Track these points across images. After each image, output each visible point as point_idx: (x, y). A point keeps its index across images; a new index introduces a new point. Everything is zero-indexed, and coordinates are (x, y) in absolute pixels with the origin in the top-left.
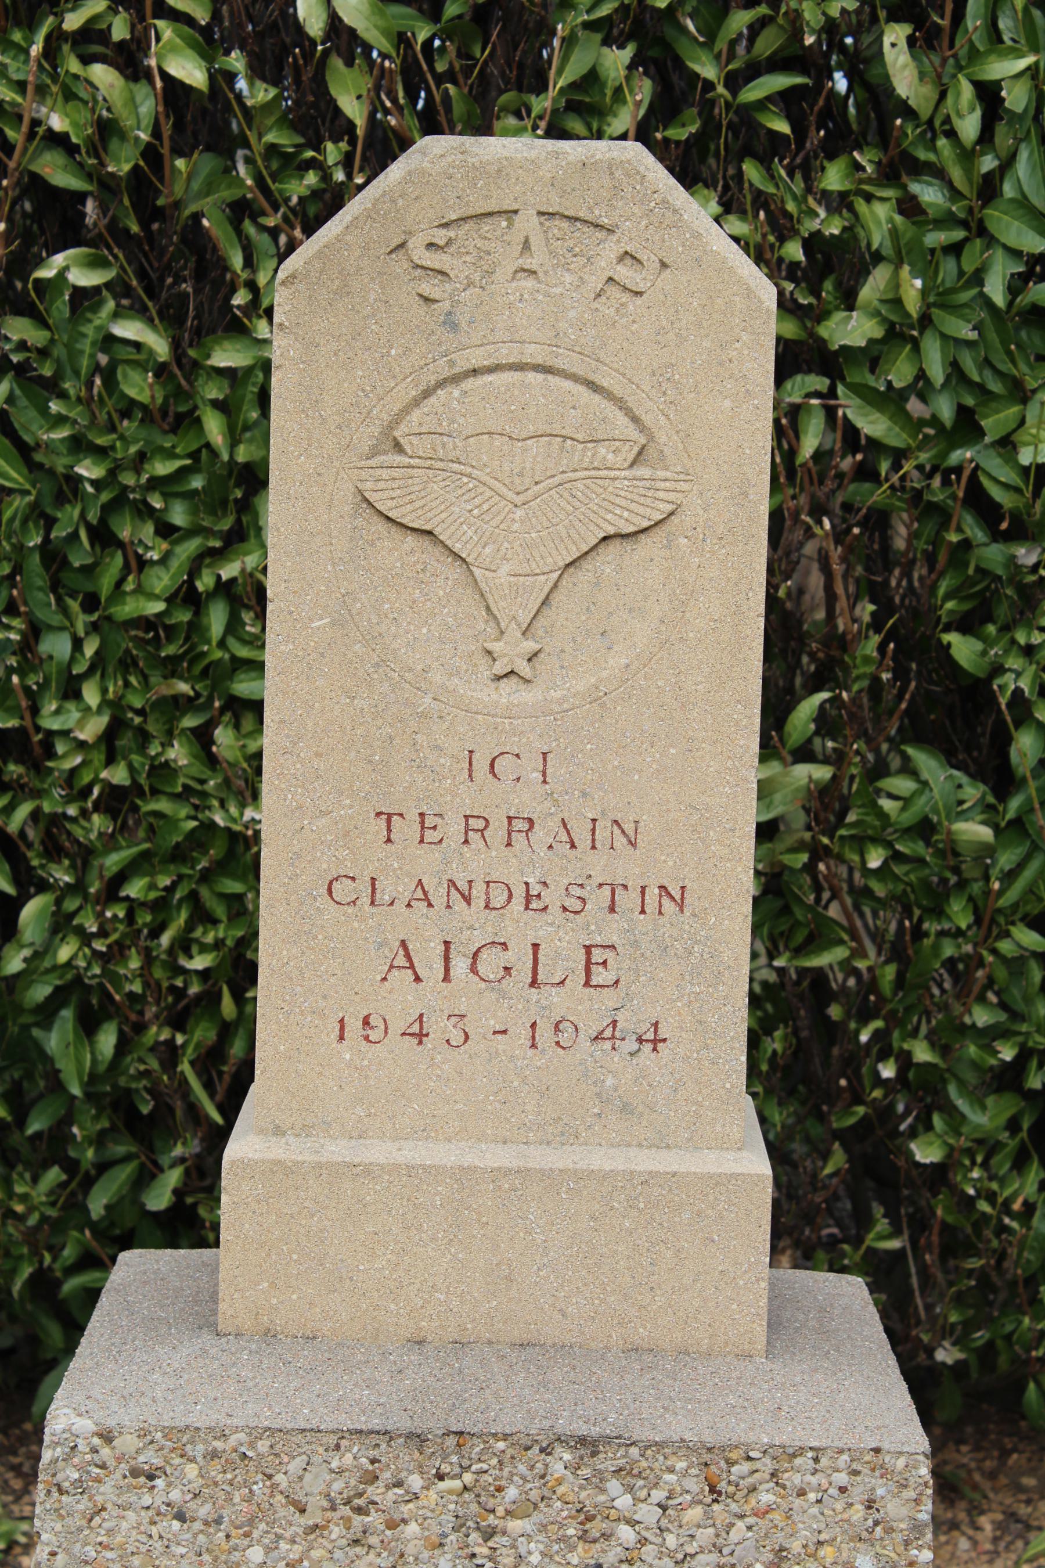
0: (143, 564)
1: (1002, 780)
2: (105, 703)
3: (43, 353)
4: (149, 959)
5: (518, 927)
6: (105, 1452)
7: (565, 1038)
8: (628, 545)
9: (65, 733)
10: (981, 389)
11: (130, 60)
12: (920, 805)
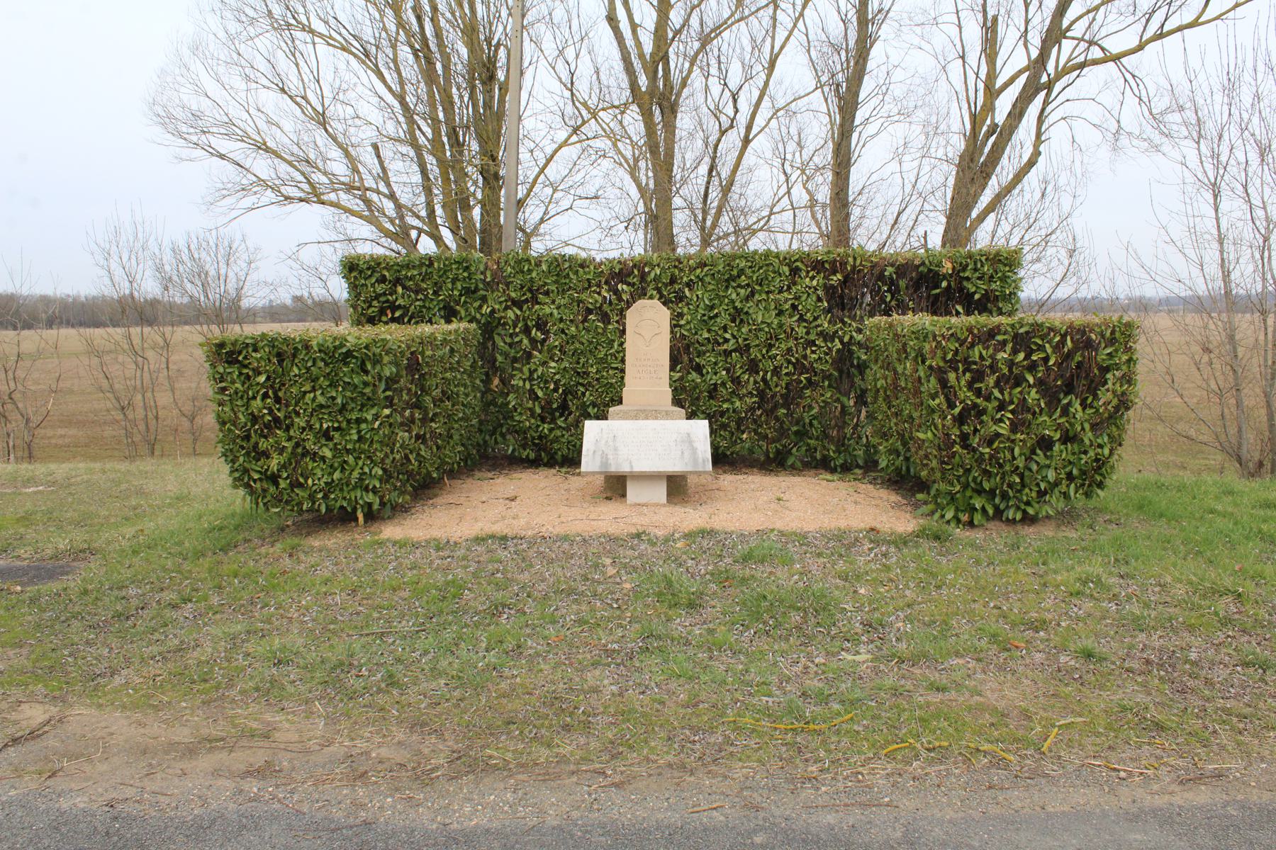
1: (702, 375)
11: (599, 293)
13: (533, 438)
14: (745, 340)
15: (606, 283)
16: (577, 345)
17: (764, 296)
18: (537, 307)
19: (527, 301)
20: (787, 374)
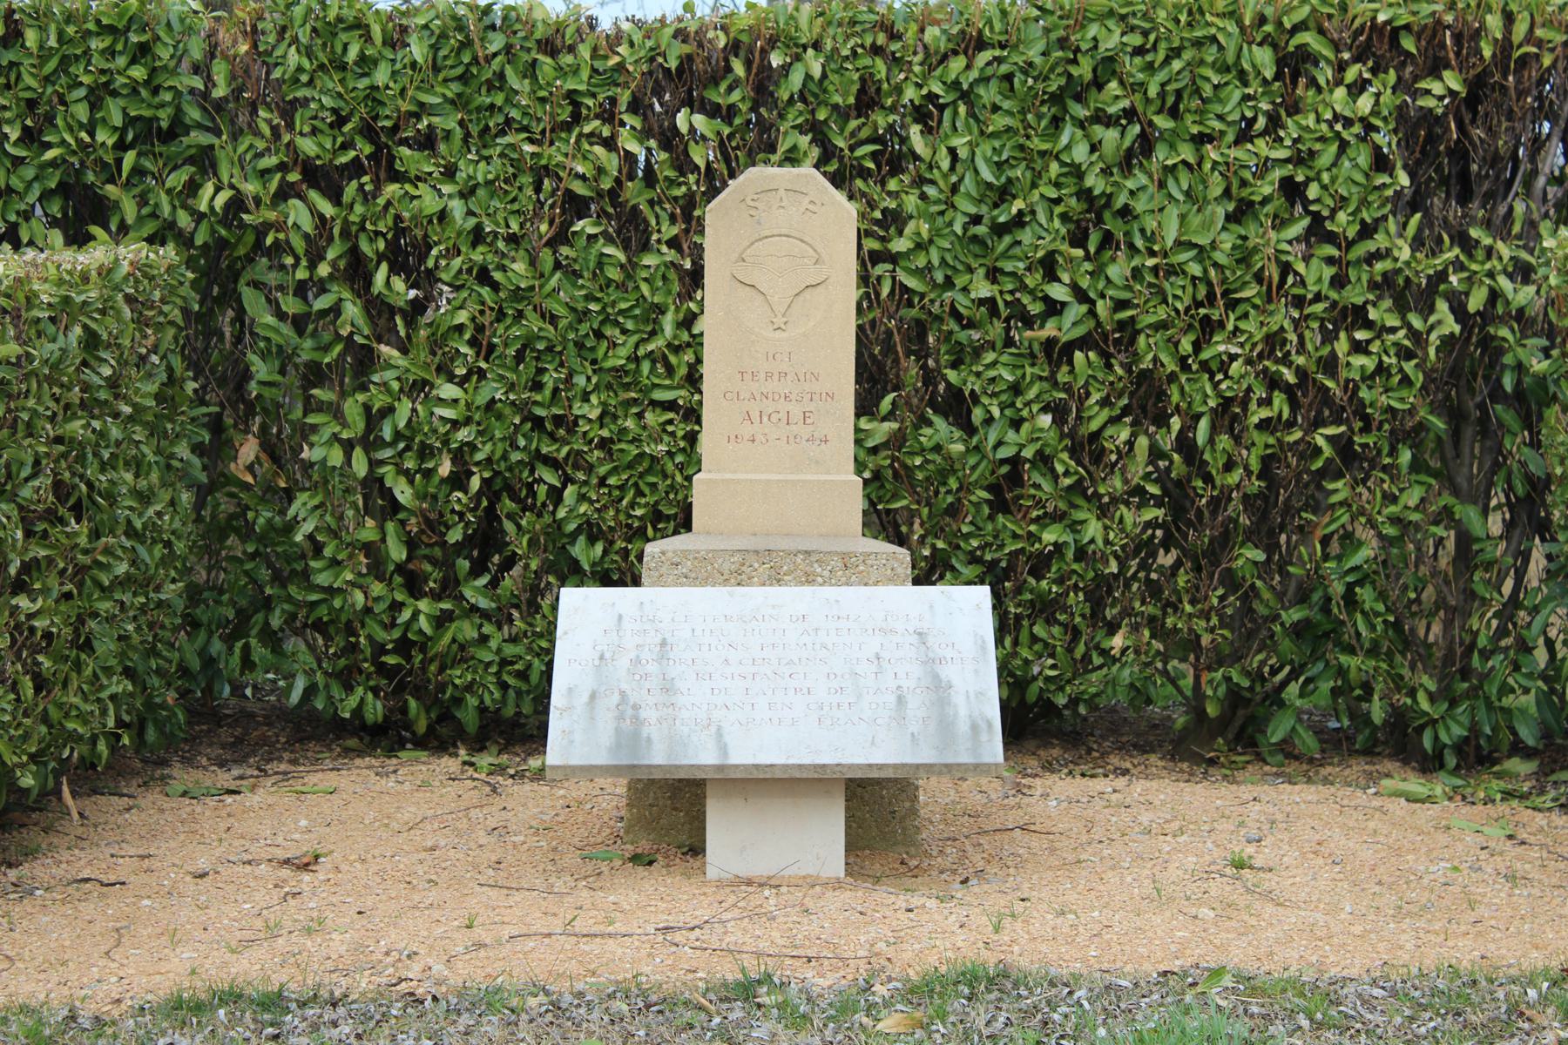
0: (615, 345)
1: (970, 430)
2: (601, 403)
3: (575, 260)
4: (618, 511)
5: (783, 406)
9: (584, 416)
10: (954, 268)
11: (610, 144)
12: (936, 438)
13: (380, 649)
14: (1121, 305)
15: (635, 106)
16: (534, 323)
17: (1187, 153)
18: (392, 189)
19: (356, 169)
20: (1264, 425)
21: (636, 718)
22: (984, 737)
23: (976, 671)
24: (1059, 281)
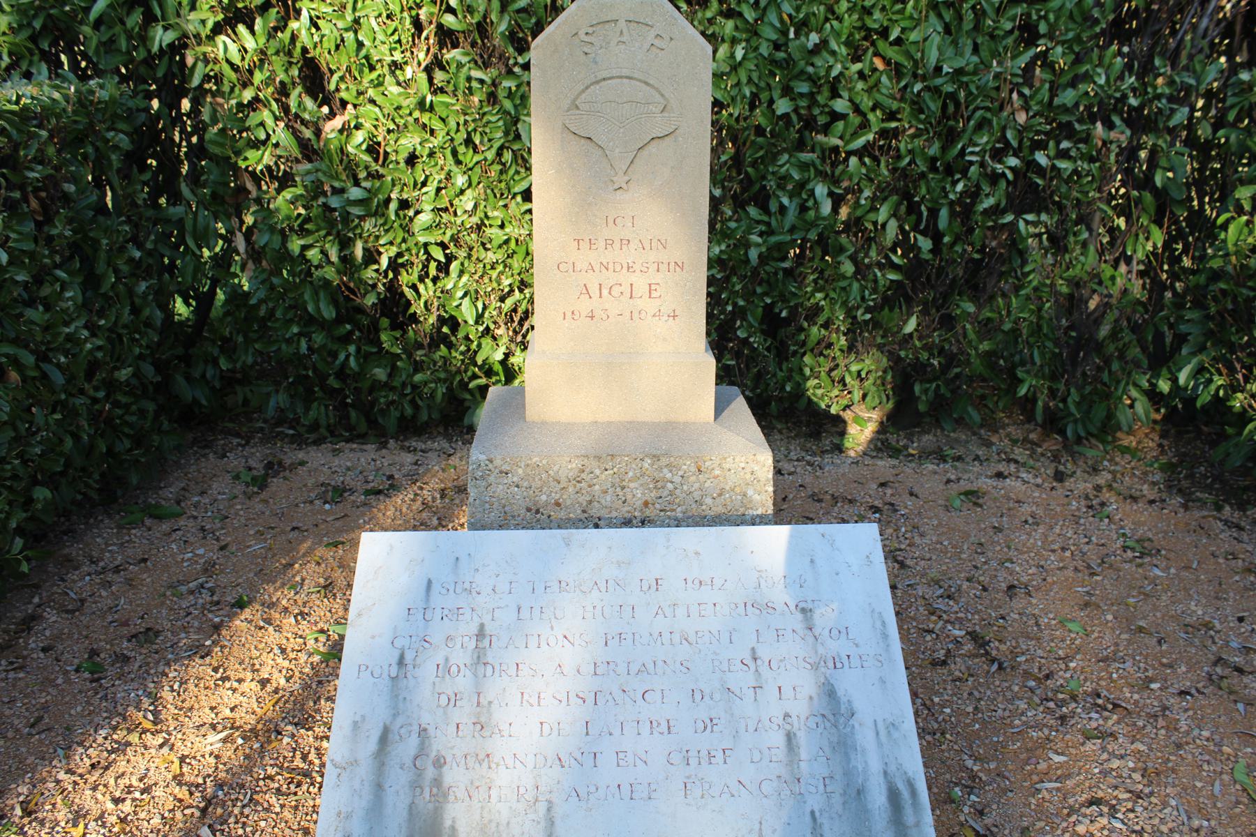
5: (626, 278)
6: (491, 466)
7: (643, 316)
8: (660, 141)
21: (437, 782)
22: (909, 818)
23: (883, 681)
24: (840, 97)
